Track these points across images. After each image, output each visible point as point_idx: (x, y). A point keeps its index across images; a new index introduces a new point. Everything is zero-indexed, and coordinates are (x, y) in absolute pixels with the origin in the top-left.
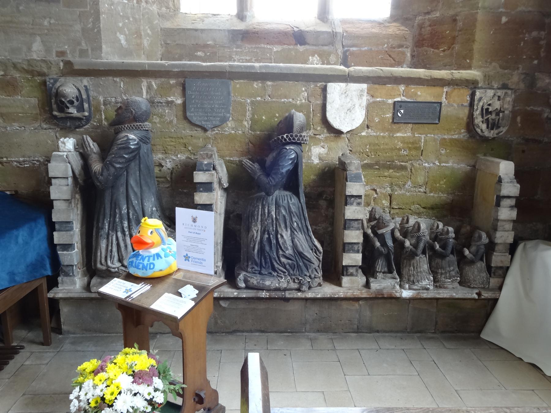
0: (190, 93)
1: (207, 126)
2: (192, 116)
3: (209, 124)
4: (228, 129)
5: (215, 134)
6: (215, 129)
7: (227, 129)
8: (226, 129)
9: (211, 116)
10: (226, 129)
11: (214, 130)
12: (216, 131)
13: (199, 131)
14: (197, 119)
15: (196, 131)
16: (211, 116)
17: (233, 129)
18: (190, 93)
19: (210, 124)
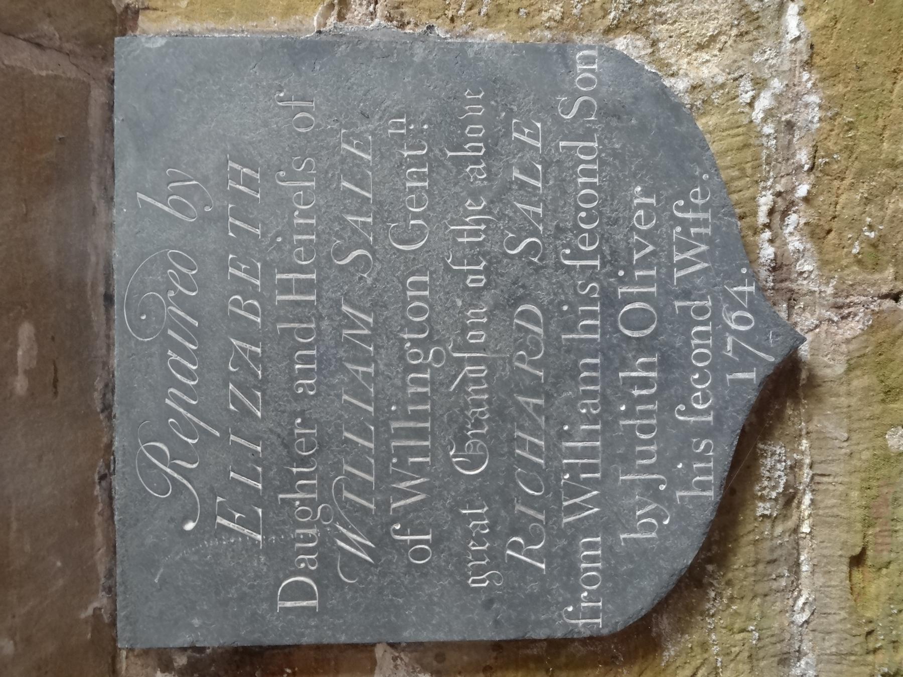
0: (303, 592)
1: (744, 361)
2: (609, 550)
3: (720, 331)
4: (760, 84)
5: (824, 263)
6: (768, 252)
7: (765, 101)
8: (758, 114)
9: (610, 302)
10: (758, 114)
11: (777, 267)
12: (795, 243)
13: (794, 468)
14: (650, 487)
15: (789, 499)
16: (610, 302)
17: (752, 17)
18: (303, 592)
19: (716, 318)
